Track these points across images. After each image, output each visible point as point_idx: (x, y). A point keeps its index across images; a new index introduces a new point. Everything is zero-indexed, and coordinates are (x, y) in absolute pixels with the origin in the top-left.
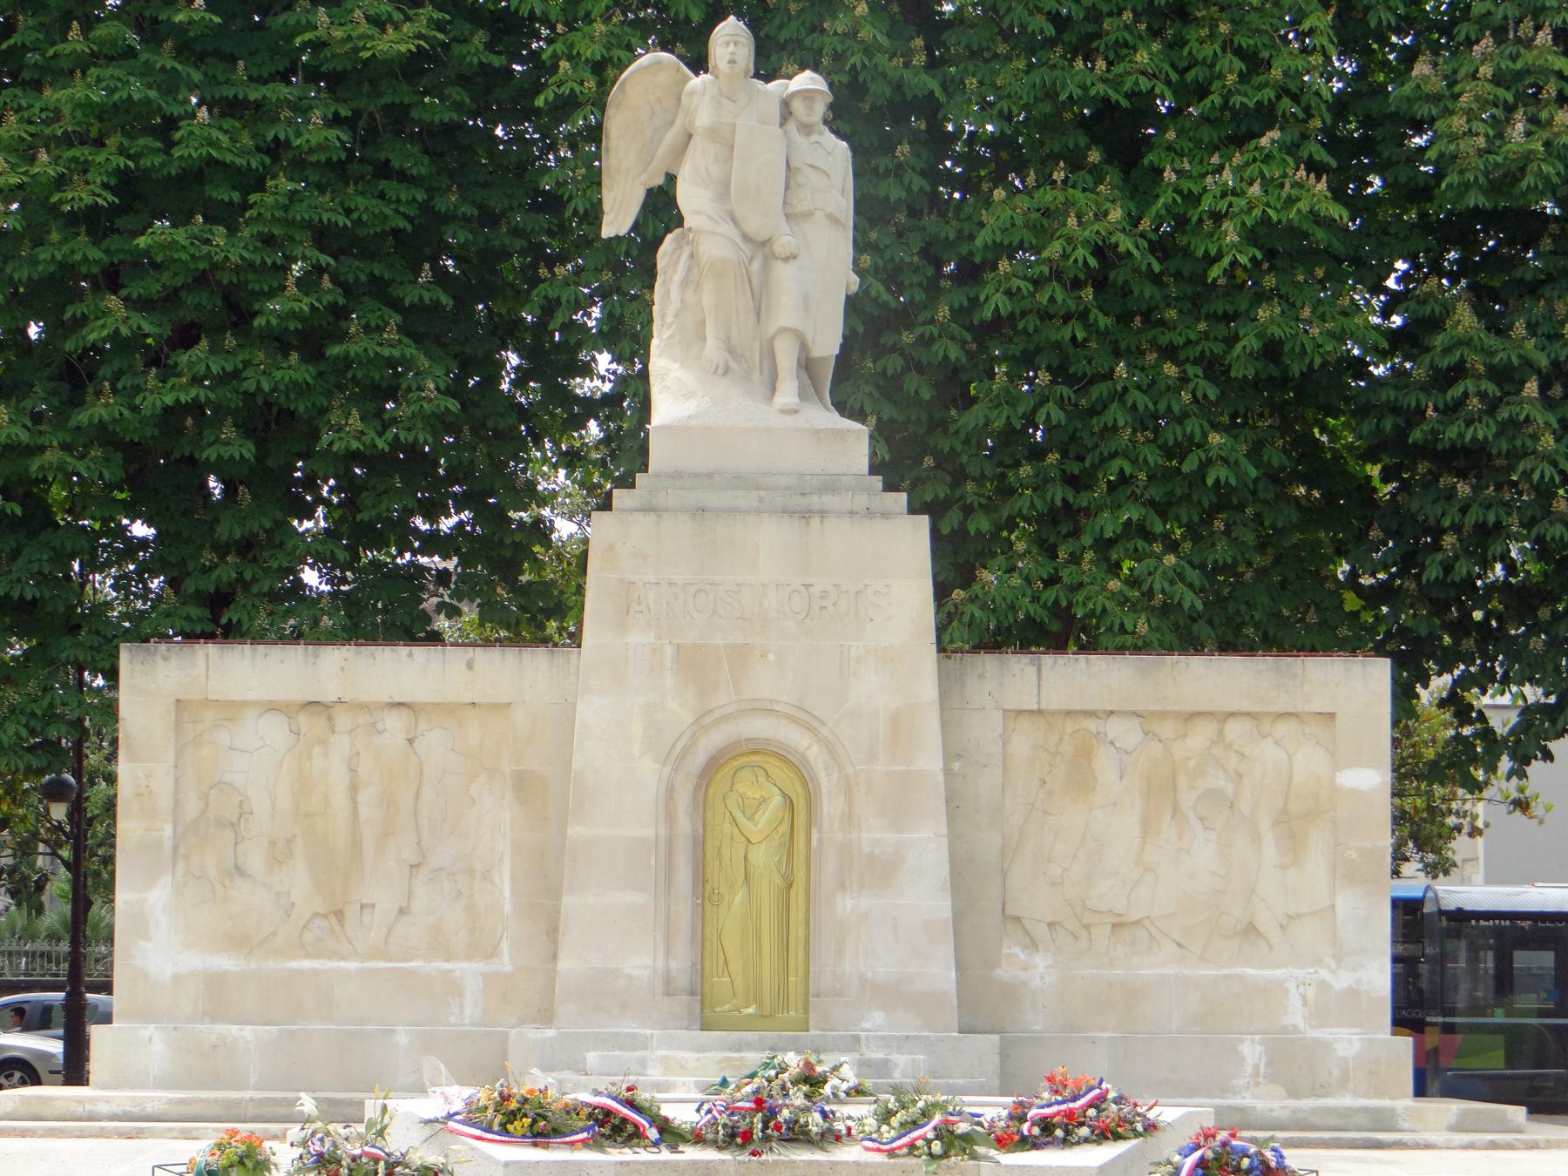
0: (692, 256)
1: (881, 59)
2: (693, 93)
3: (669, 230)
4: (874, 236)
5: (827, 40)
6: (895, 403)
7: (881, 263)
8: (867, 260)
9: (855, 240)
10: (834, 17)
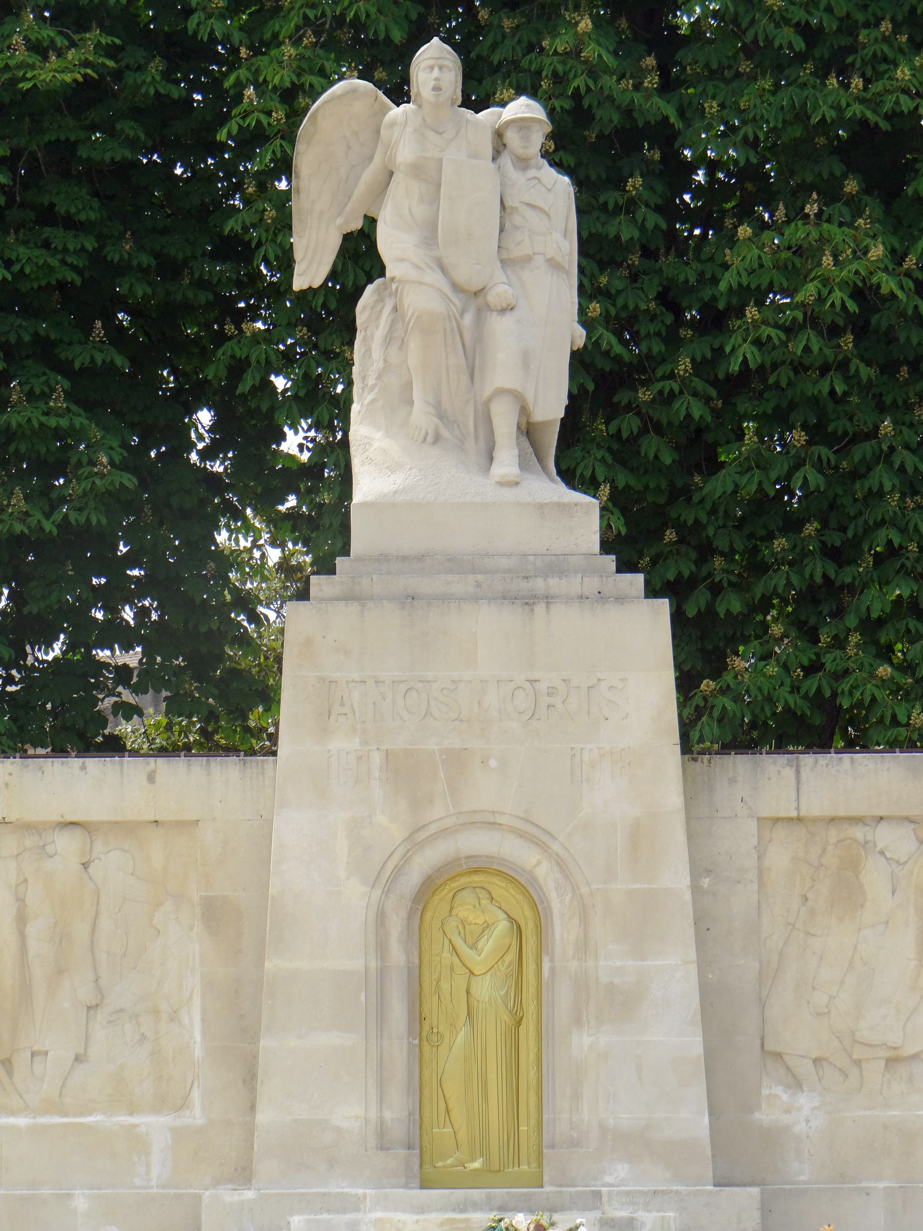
0: (395, 309)
1: (609, 81)
2: (393, 124)
3: (370, 280)
4: (604, 280)
5: (547, 61)
6: (632, 470)
7: (613, 312)
8: (595, 308)
9: (581, 287)
10: (554, 34)
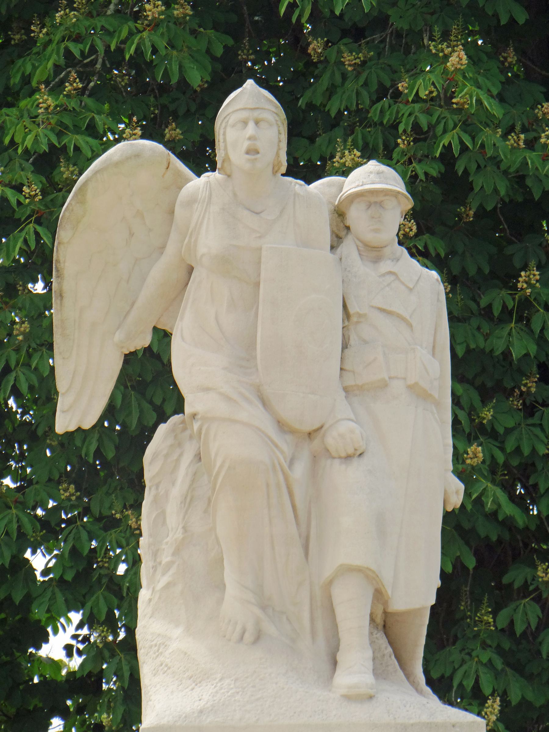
0: (198, 457)
1: (491, 137)
2: (192, 201)
3: (163, 418)
4: (487, 414)
5: (405, 110)
6: (530, 678)
7: (501, 458)
8: (476, 453)
9: (456, 422)
10: (415, 72)
